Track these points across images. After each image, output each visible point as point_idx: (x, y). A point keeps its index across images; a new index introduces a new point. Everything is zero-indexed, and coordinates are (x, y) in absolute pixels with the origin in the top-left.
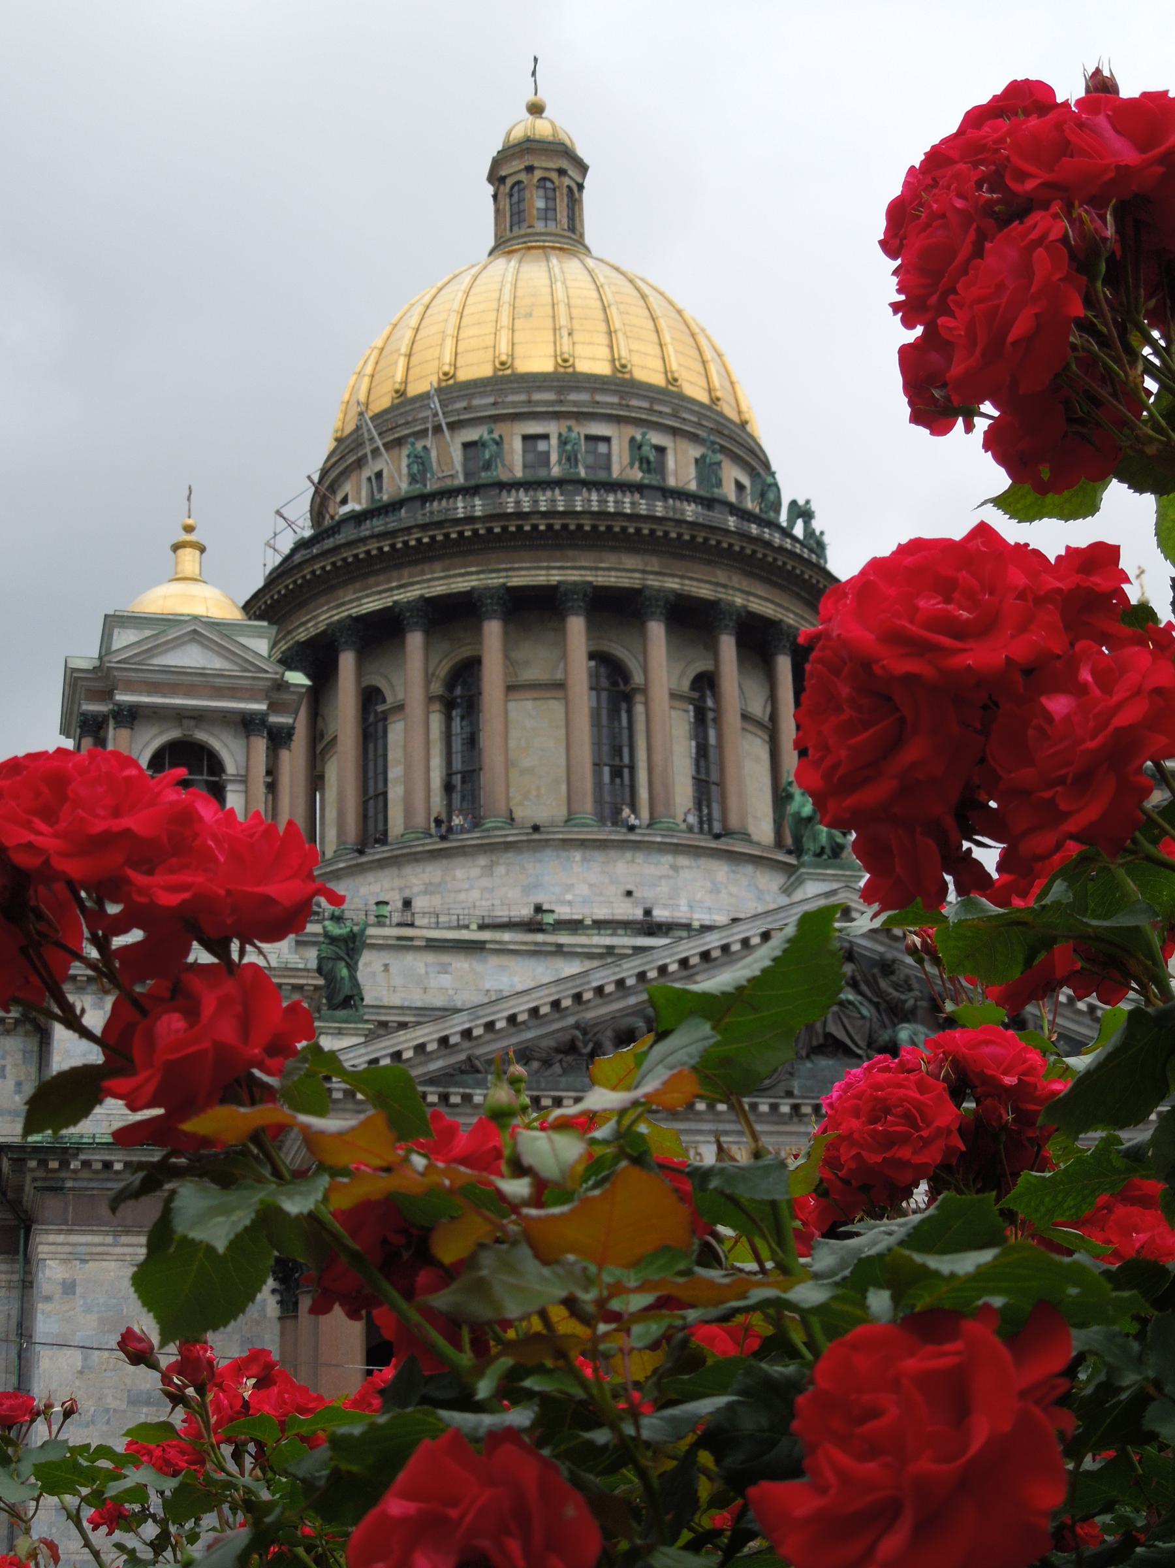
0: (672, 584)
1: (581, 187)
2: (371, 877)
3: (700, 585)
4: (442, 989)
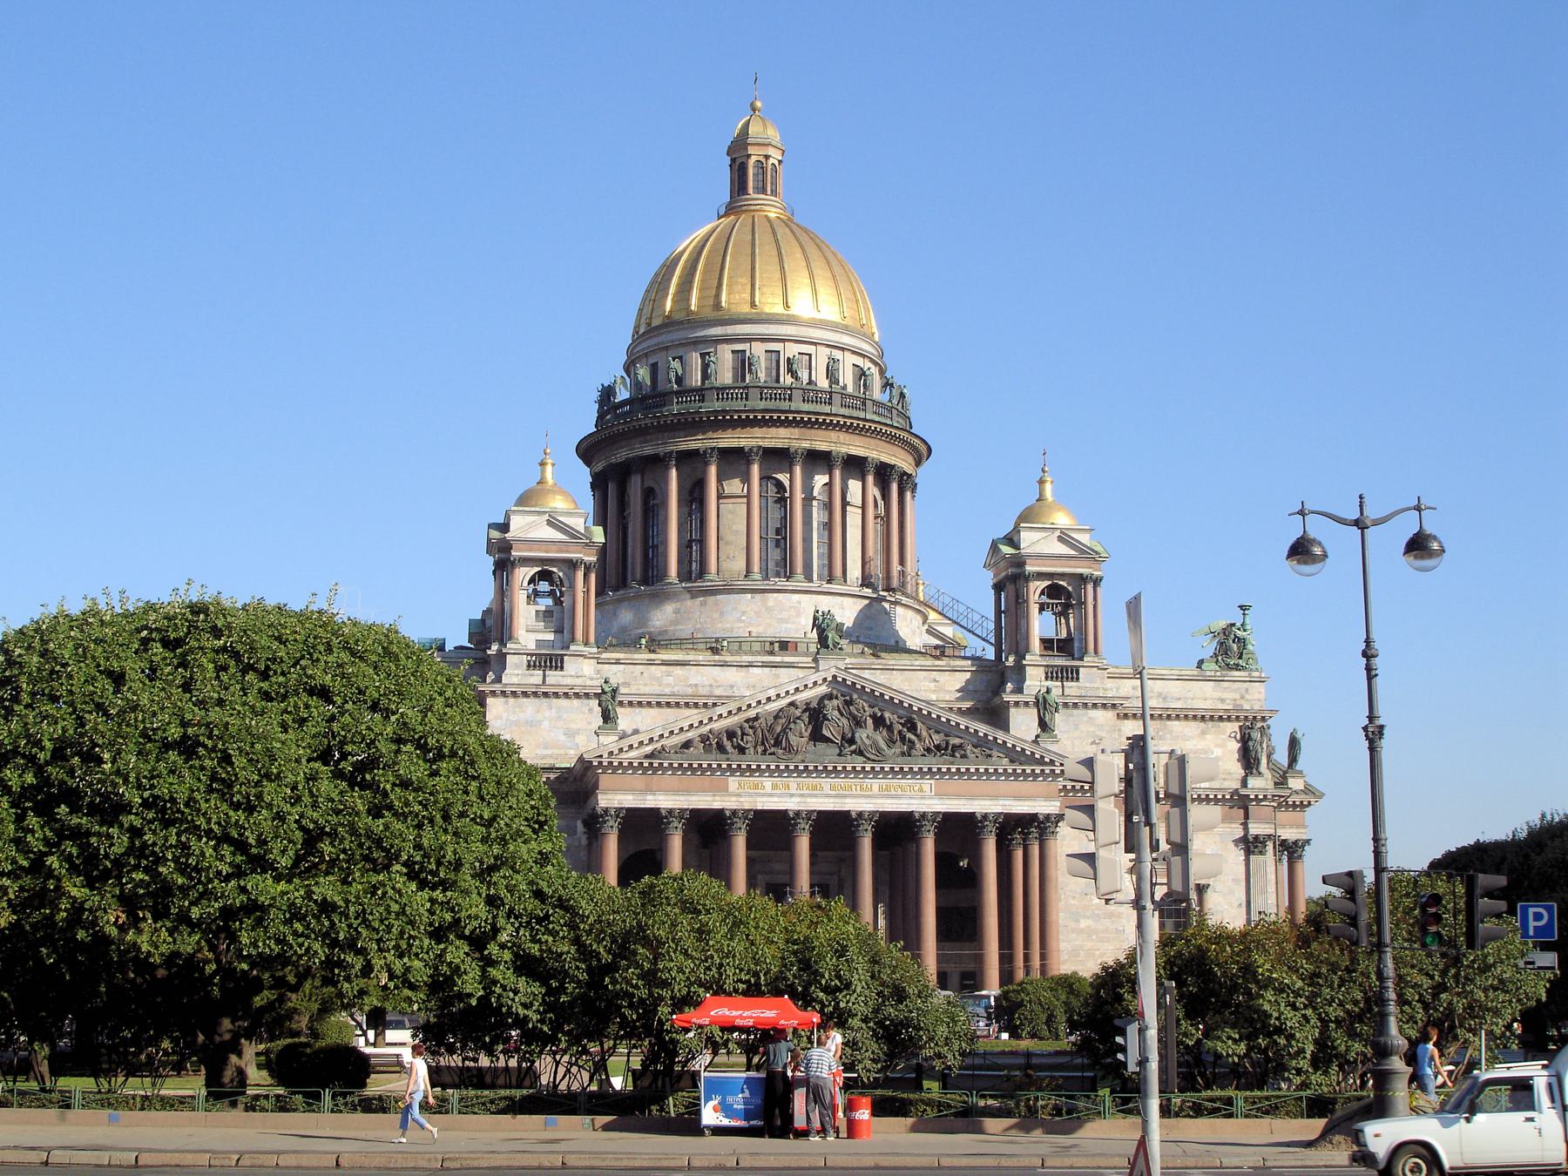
0: (806, 445)
3: (822, 441)
4: (669, 685)
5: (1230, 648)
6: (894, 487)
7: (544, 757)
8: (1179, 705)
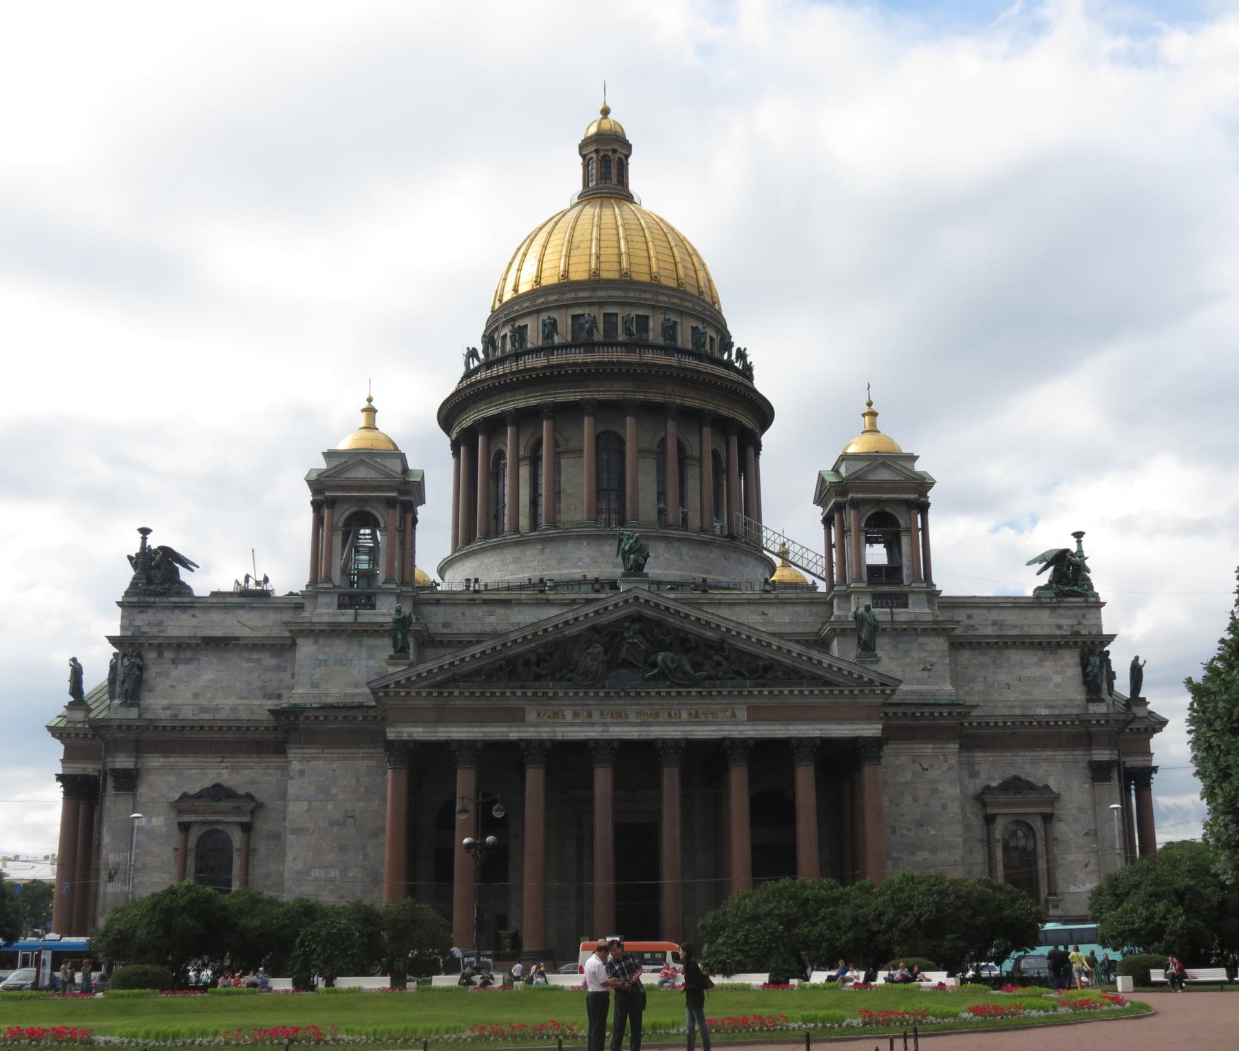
0: (640, 396)
1: (627, 157)
2: (489, 554)
5: (1065, 575)
6: (734, 441)
7: (356, 694)
8: (1015, 632)
